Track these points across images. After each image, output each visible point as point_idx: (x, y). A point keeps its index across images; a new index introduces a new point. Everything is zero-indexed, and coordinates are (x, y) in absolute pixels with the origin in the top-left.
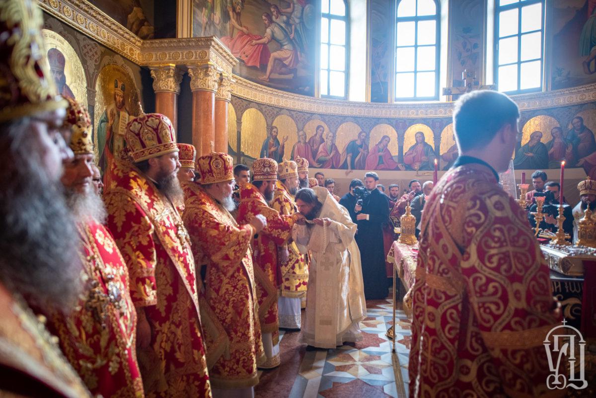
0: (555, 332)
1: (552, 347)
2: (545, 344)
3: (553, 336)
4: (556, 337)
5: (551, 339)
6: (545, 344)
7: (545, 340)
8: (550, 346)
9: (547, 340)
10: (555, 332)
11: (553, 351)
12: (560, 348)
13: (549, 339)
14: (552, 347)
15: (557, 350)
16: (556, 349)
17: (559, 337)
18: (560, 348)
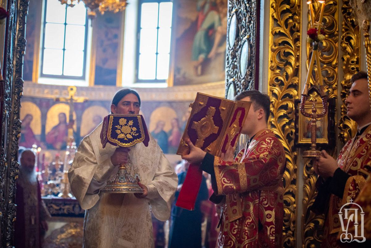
0: (346, 207)
1: (343, 216)
2: (339, 215)
3: (345, 209)
4: (346, 210)
5: (343, 211)
6: (339, 215)
7: (339, 212)
8: (342, 215)
9: (340, 212)
10: (346, 207)
11: (345, 218)
12: (349, 216)
13: (342, 211)
14: (343, 216)
15: (347, 218)
16: (346, 217)
17: (348, 210)
18: (349, 216)
